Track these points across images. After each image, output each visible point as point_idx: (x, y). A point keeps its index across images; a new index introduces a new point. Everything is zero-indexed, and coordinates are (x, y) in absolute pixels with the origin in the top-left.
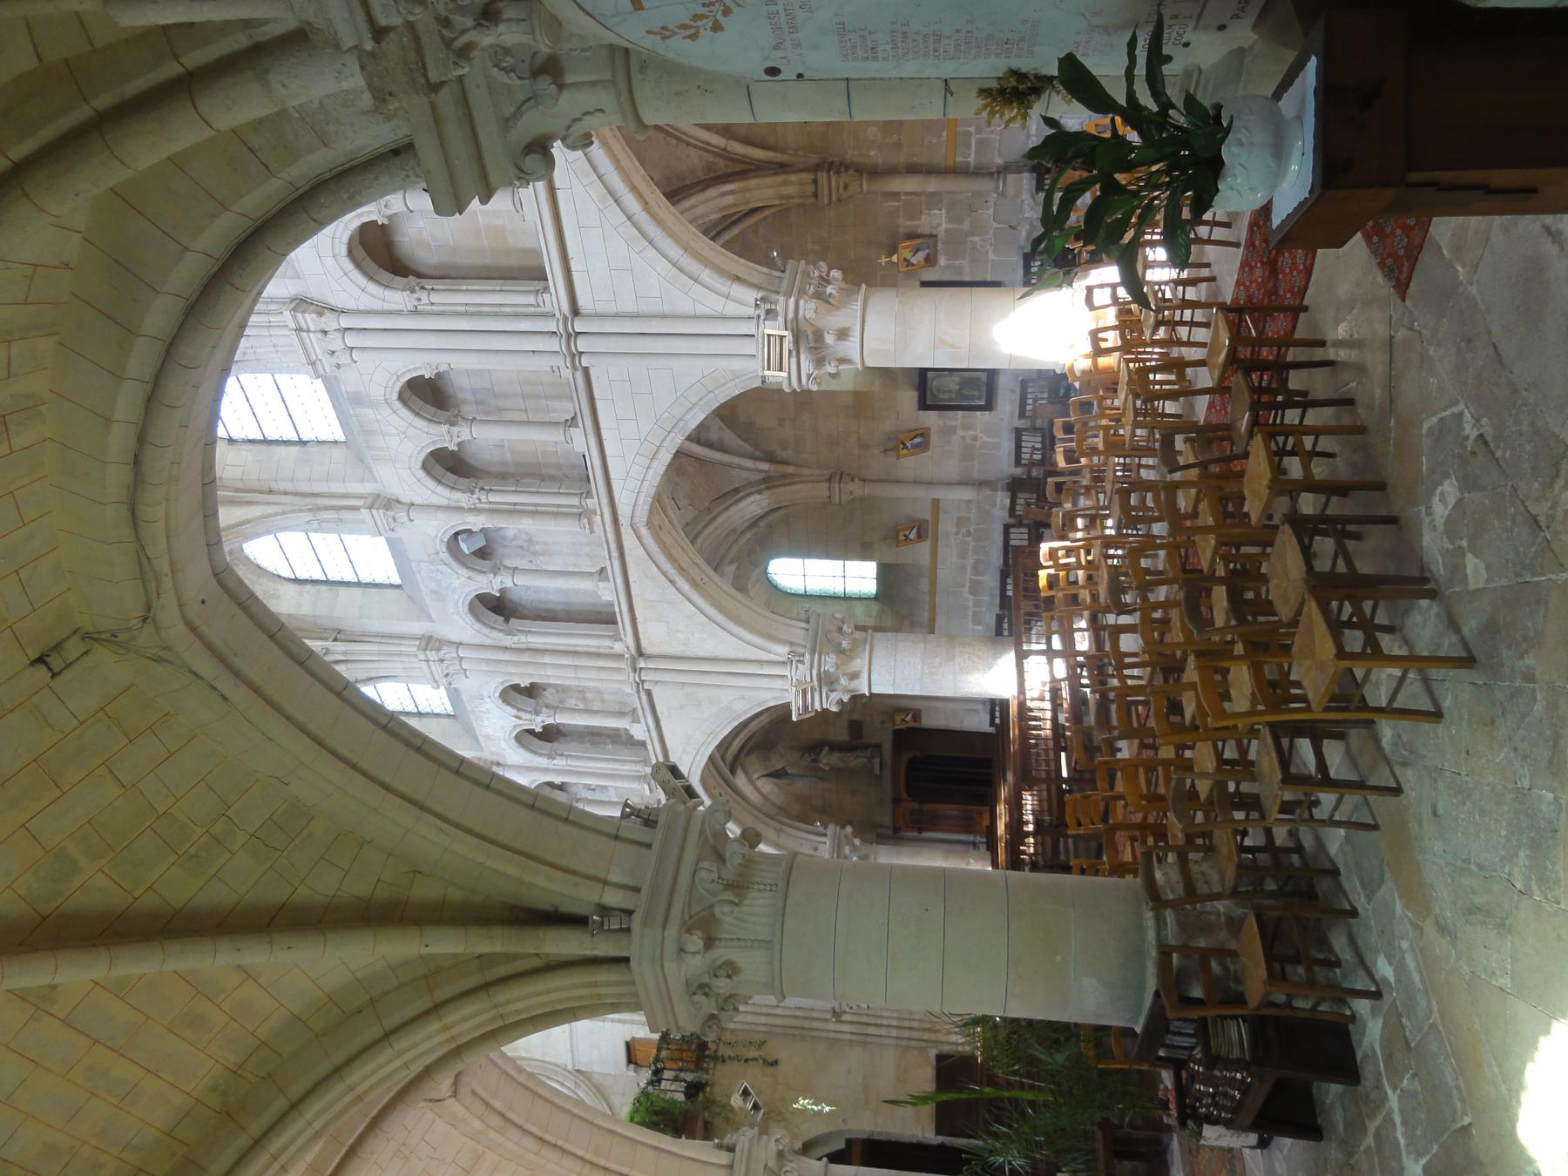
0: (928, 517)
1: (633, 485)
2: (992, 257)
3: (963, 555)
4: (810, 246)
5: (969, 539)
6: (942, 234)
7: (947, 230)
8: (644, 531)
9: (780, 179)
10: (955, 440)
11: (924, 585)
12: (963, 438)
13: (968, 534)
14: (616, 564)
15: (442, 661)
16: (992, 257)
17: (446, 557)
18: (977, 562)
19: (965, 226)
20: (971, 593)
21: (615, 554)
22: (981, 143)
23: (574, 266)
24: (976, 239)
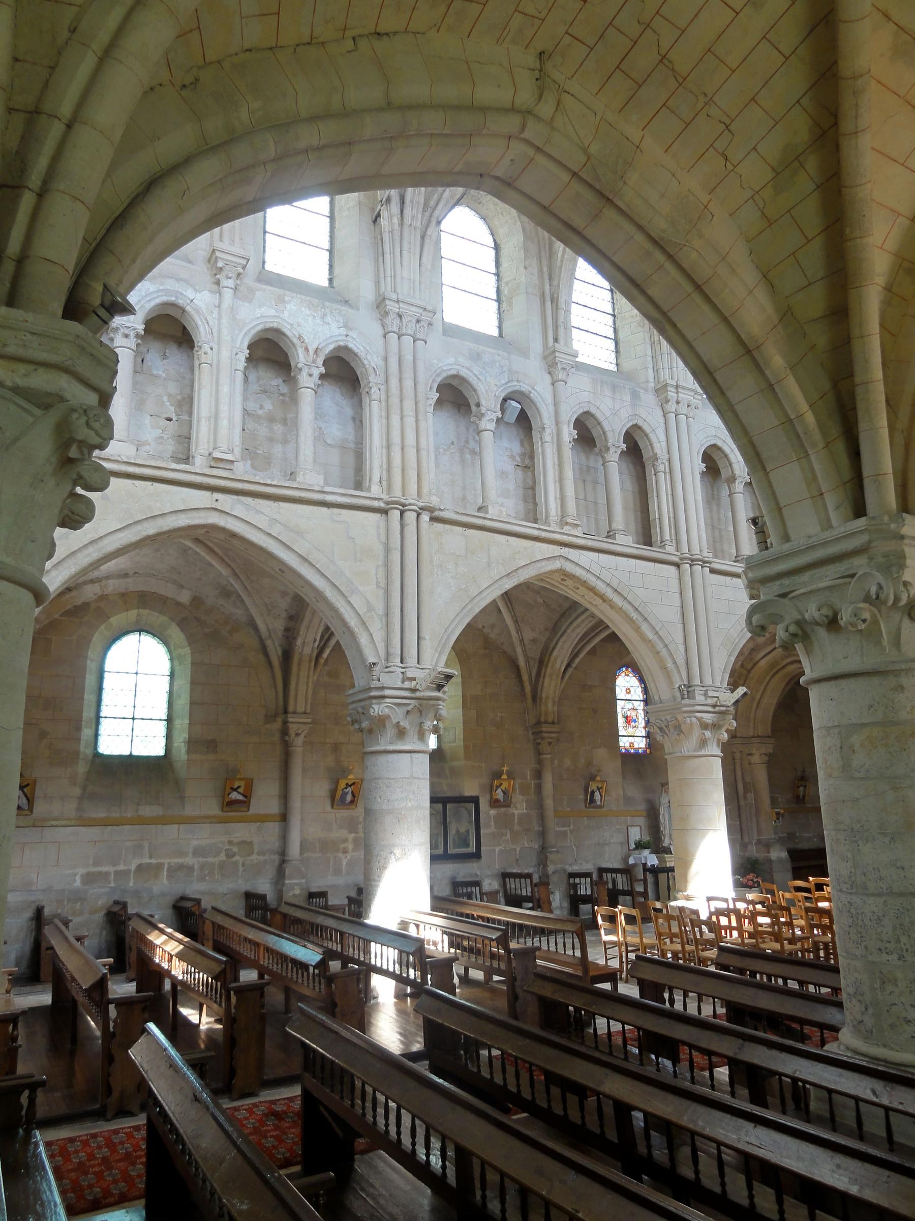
0: (253, 810)
1: (596, 570)
2: (497, 849)
3: (197, 852)
4: (499, 714)
5: (222, 857)
6: (512, 810)
7: (513, 814)
8: (557, 565)
9: (556, 699)
10: (344, 833)
11: (147, 811)
12: (345, 841)
13: (230, 855)
14: (536, 533)
15: (418, 321)
16: (497, 849)
17: (515, 386)
18: (191, 869)
19: (516, 828)
20: (140, 868)
21: (544, 535)
22: (564, 834)
23: (728, 579)
24: (508, 836)
